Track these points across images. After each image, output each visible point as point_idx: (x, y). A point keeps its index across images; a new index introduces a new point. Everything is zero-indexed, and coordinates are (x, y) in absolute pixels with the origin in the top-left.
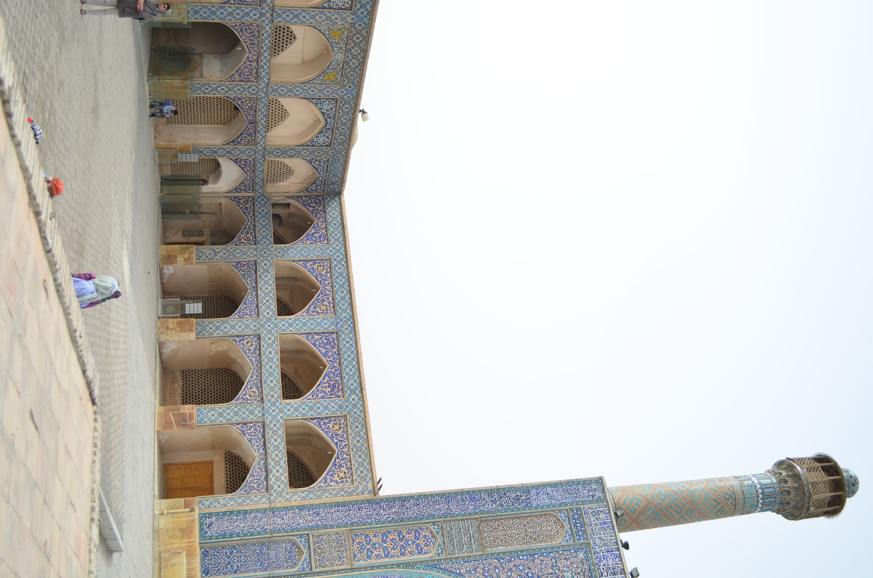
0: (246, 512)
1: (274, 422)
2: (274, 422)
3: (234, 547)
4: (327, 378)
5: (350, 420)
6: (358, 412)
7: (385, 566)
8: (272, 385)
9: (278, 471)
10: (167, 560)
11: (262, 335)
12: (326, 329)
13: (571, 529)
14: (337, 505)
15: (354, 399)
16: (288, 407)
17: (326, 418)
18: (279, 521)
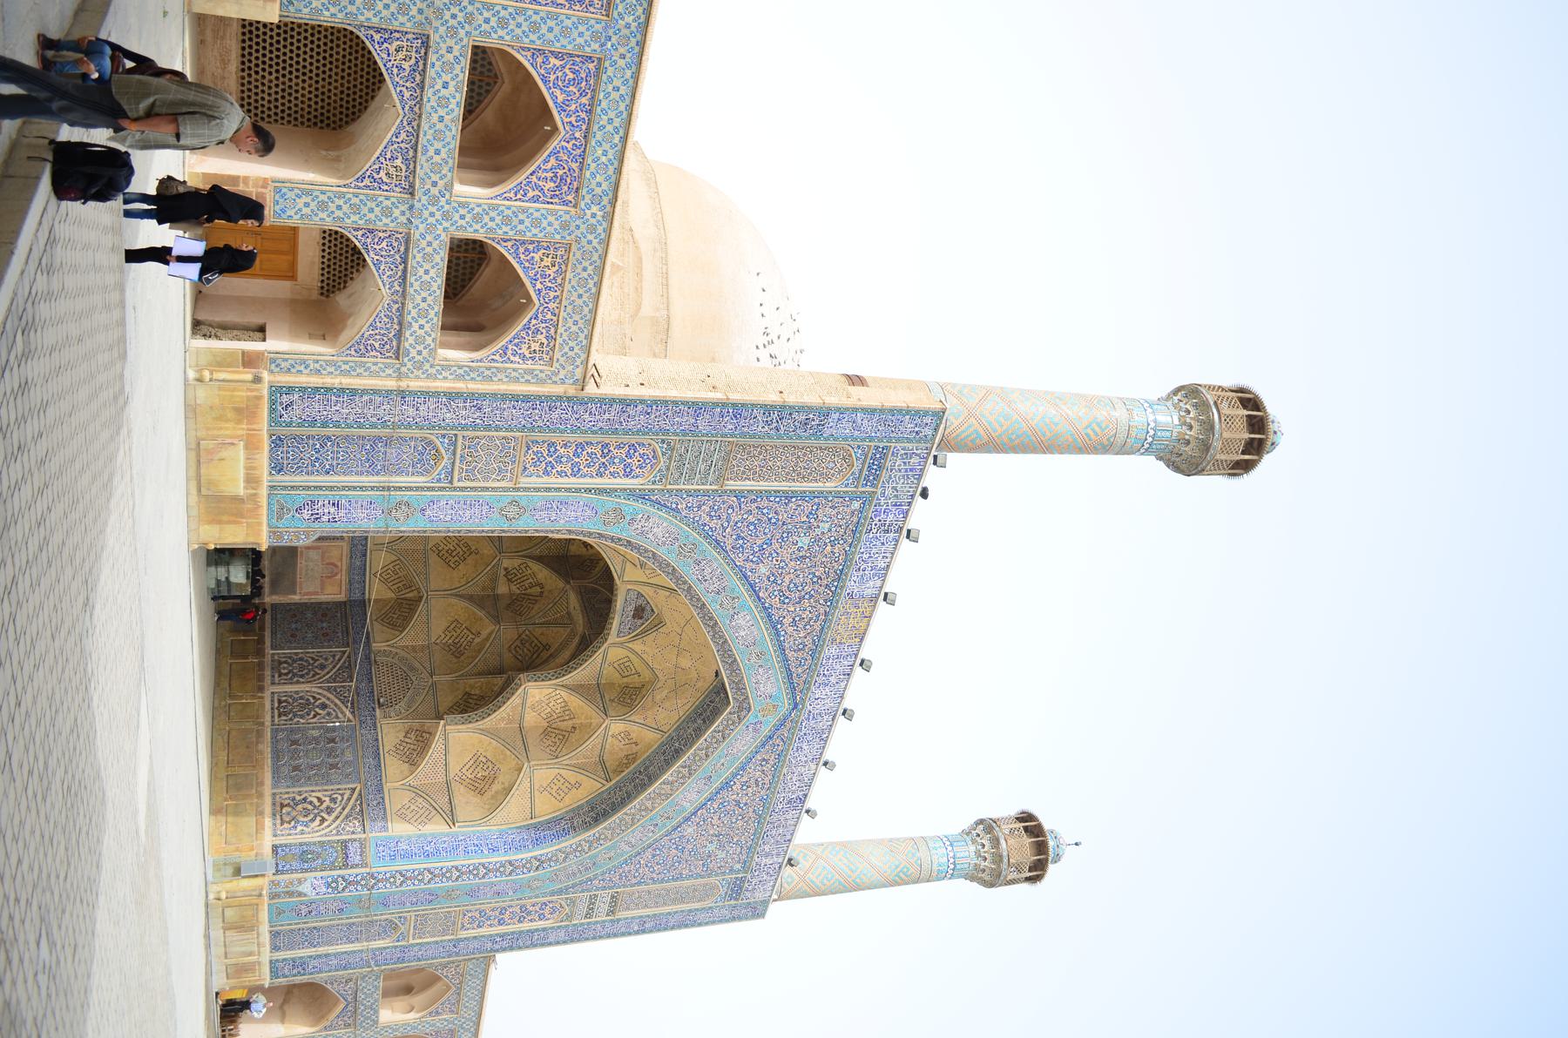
0: (354, 392)
1: (428, 238)
2: (428, 238)
3: (329, 438)
4: (553, 161)
5: (576, 253)
6: (595, 242)
7: (568, 490)
8: (437, 158)
9: (421, 327)
10: (209, 452)
11: (434, 38)
12: (581, 47)
13: (861, 471)
14: (515, 398)
15: (594, 215)
16: (462, 211)
17: (532, 242)
18: (412, 412)
